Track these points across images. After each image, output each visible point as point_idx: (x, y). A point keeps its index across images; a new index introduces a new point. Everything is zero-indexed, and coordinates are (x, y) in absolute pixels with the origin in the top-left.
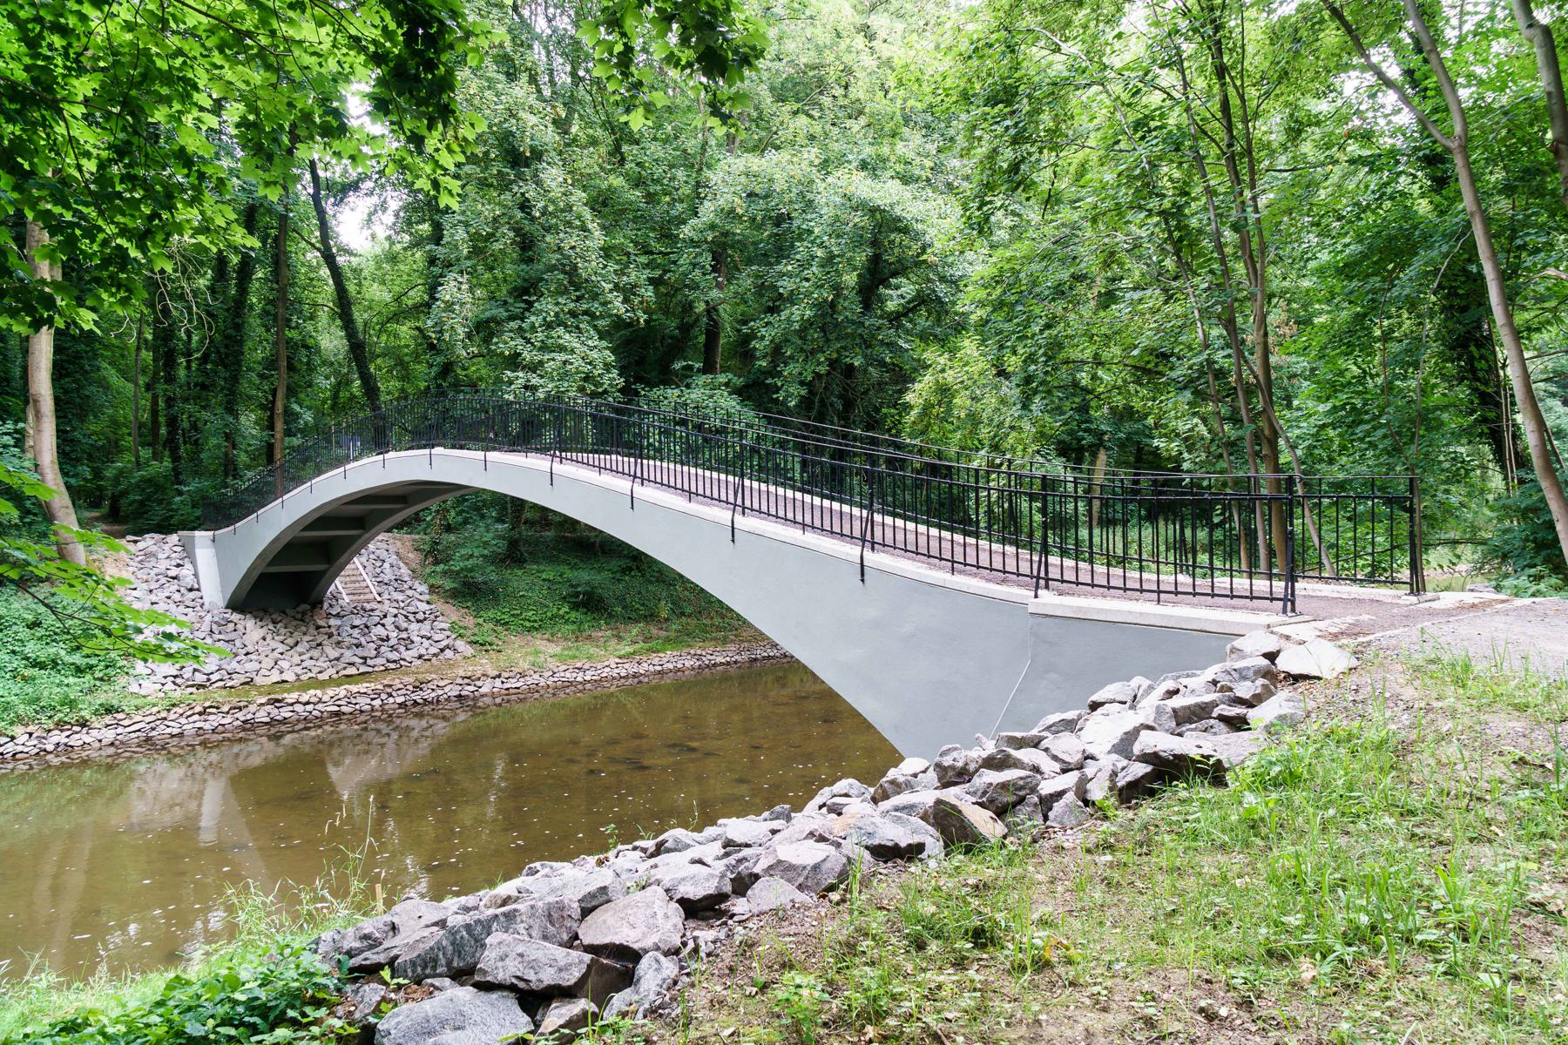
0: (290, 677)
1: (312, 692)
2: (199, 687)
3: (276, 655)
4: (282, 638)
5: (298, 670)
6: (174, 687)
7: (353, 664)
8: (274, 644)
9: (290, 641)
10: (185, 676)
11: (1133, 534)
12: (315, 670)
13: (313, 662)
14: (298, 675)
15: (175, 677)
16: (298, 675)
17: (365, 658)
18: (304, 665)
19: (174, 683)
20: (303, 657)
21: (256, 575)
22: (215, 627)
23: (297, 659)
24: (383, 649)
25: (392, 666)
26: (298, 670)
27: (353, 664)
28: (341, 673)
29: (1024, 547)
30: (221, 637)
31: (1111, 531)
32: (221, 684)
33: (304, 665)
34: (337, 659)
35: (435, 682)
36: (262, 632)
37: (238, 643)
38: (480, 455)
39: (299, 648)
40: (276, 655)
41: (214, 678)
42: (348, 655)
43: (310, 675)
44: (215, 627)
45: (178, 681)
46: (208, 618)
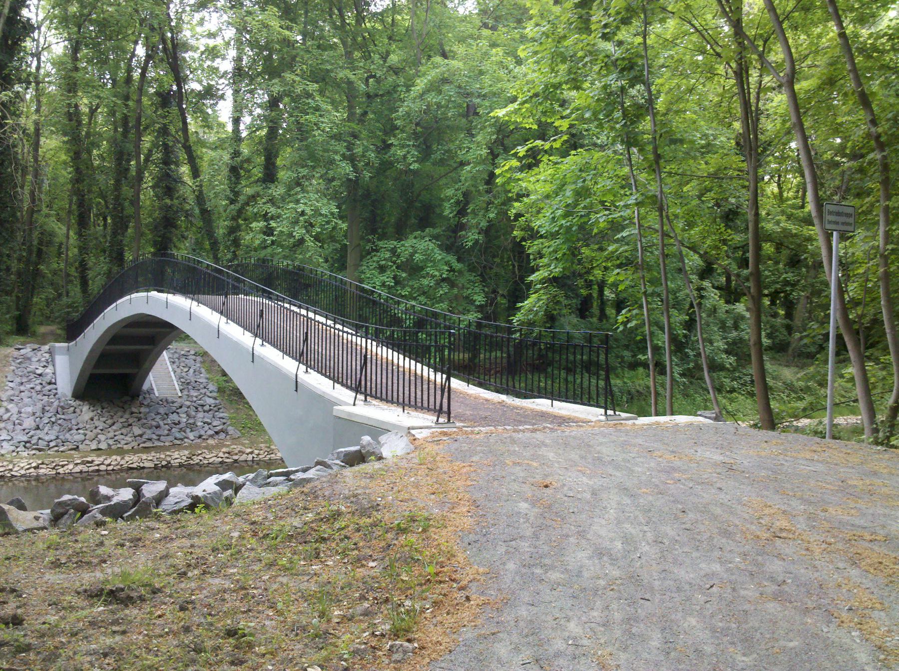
0: (103, 446)
1: (114, 457)
2: (40, 450)
3: (98, 431)
4: (104, 419)
5: (111, 442)
6: (23, 449)
7: (150, 440)
8: (97, 423)
9: (110, 422)
10: (33, 442)
11: (578, 376)
12: (123, 442)
13: (122, 437)
14: (109, 445)
15: (26, 442)
16: (109, 445)
17: (160, 436)
18: (116, 438)
19: (25, 447)
20: (117, 433)
21: (87, 374)
22: (60, 409)
23: (111, 434)
24: (174, 430)
25: (178, 442)
26: (111, 442)
27: (150, 440)
28: (142, 445)
29: (361, 393)
30: (63, 417)
31: (523, 379)
32: (56, 448)
33: (116, 438)
34: (141, 436)
35: (204, 455)
36: (91, 414)
37: (74, 422)
38: (145, 294)
39: (114, 427)
40: (98, 431)
41: (52, 444)
42: (149, 433)
43: (119, 446)
44: (60, 409)
45: (28, 445)
46: (56, 403)
